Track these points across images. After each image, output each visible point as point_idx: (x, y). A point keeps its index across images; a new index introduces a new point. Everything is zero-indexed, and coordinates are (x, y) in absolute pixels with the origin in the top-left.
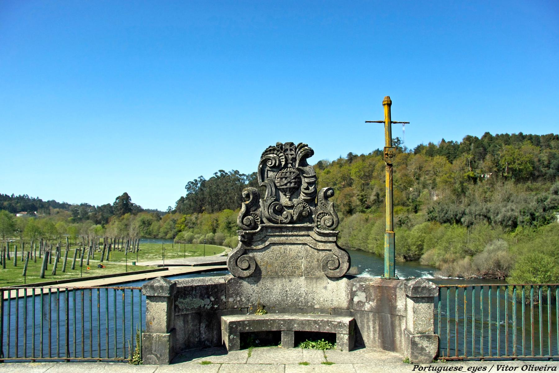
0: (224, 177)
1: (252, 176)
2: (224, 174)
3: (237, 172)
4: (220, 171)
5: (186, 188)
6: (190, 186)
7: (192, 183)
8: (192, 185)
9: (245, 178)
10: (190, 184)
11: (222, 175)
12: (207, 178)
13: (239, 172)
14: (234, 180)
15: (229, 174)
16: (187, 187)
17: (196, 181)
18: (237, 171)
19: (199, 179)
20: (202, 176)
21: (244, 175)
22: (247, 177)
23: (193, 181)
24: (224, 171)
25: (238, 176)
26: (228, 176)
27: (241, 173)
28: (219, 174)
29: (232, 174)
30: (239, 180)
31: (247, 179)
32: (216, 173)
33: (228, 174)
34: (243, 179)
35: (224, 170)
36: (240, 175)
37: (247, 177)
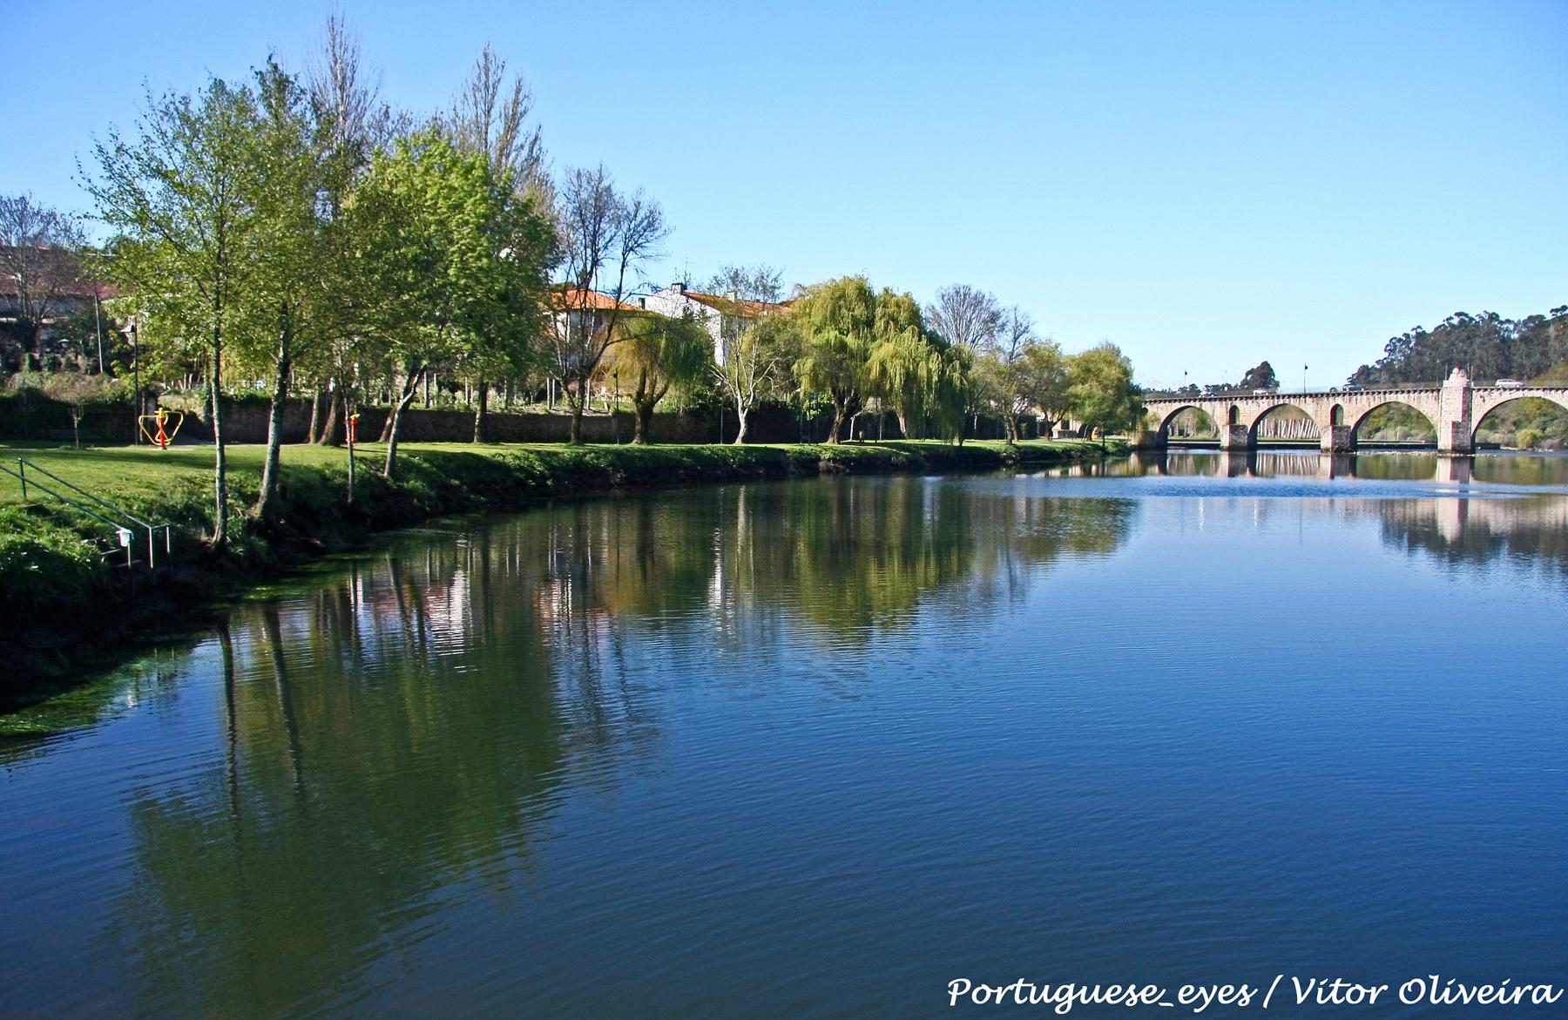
0: (1466, 327)
1: (1525, 322)
2: (1467, 319)
3: (1494, 317)
4: (1458, 314)
5: (1385, 350)
6: (1395, 346)
7: (1400, 340)
8: (1398, 344)
9: (1511, 327)
10: (1394, 343)
11: (1462, 322)
12: (1429, 330)
13: (1497, 316)
14: (1488, 334)
15: (1477, 319)
16: (1388, 348)
17: (1407, 336)
18: (1494, 313)
19: (1414, 333)
20: (1419, 327)
21: (1508, 321)
22: (1516, 325)
23: (1400, 336)
24: (1466, 315)
25: (1496, 323)
26: (1474, 325)
27: (1502, 318)
28: (1455, 321)
29: (1483, 319)
30: (1497, 332)
31: (1514, 329)
32: (1451, 318)
33: (1474, 319)
34: (1507, 330)
35: (1466, 312)
36: (1501, 323)
37: (1516, 325)
